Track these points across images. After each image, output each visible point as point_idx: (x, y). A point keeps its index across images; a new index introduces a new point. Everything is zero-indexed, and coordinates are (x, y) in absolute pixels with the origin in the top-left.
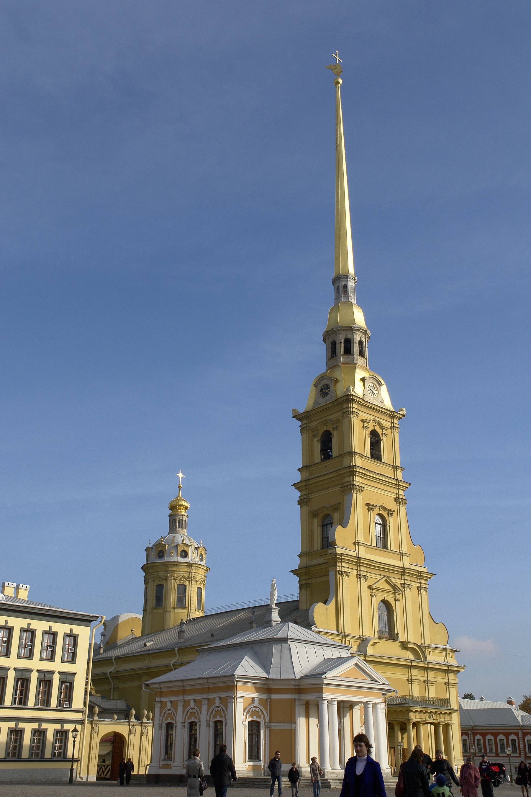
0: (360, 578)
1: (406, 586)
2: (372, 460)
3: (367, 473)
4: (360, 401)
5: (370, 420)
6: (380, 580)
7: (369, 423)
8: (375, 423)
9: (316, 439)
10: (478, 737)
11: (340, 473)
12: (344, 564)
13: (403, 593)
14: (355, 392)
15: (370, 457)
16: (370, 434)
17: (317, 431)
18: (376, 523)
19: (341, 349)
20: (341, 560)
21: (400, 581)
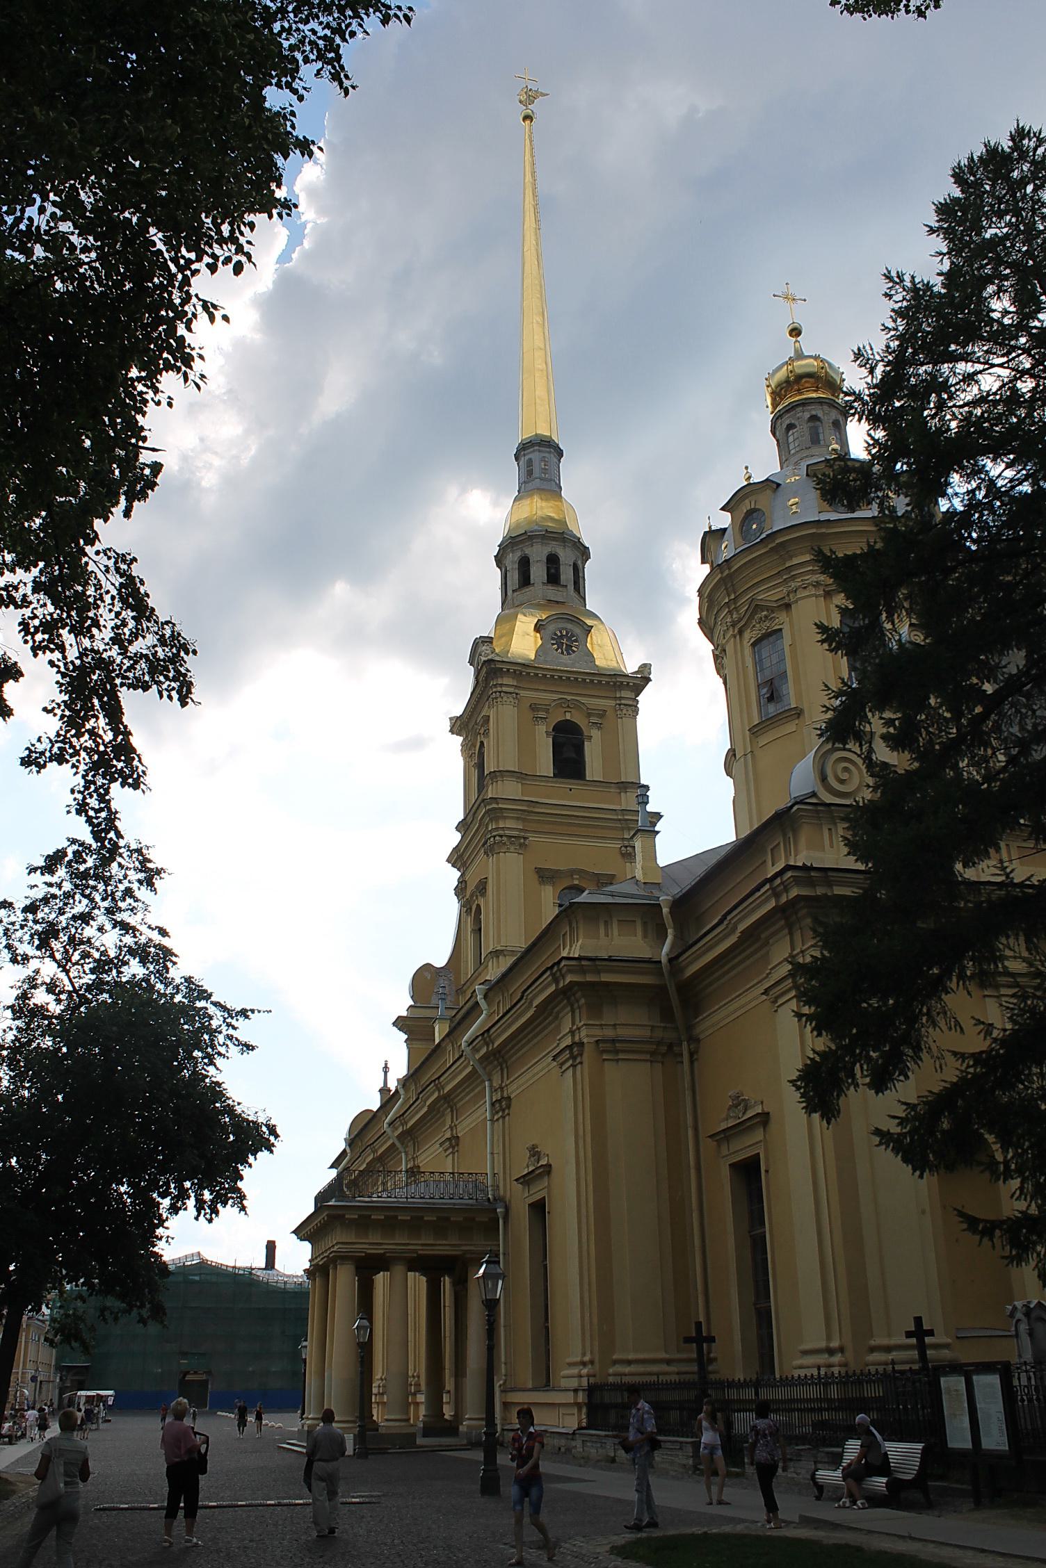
2: (555, 779)
8: (568, 706)
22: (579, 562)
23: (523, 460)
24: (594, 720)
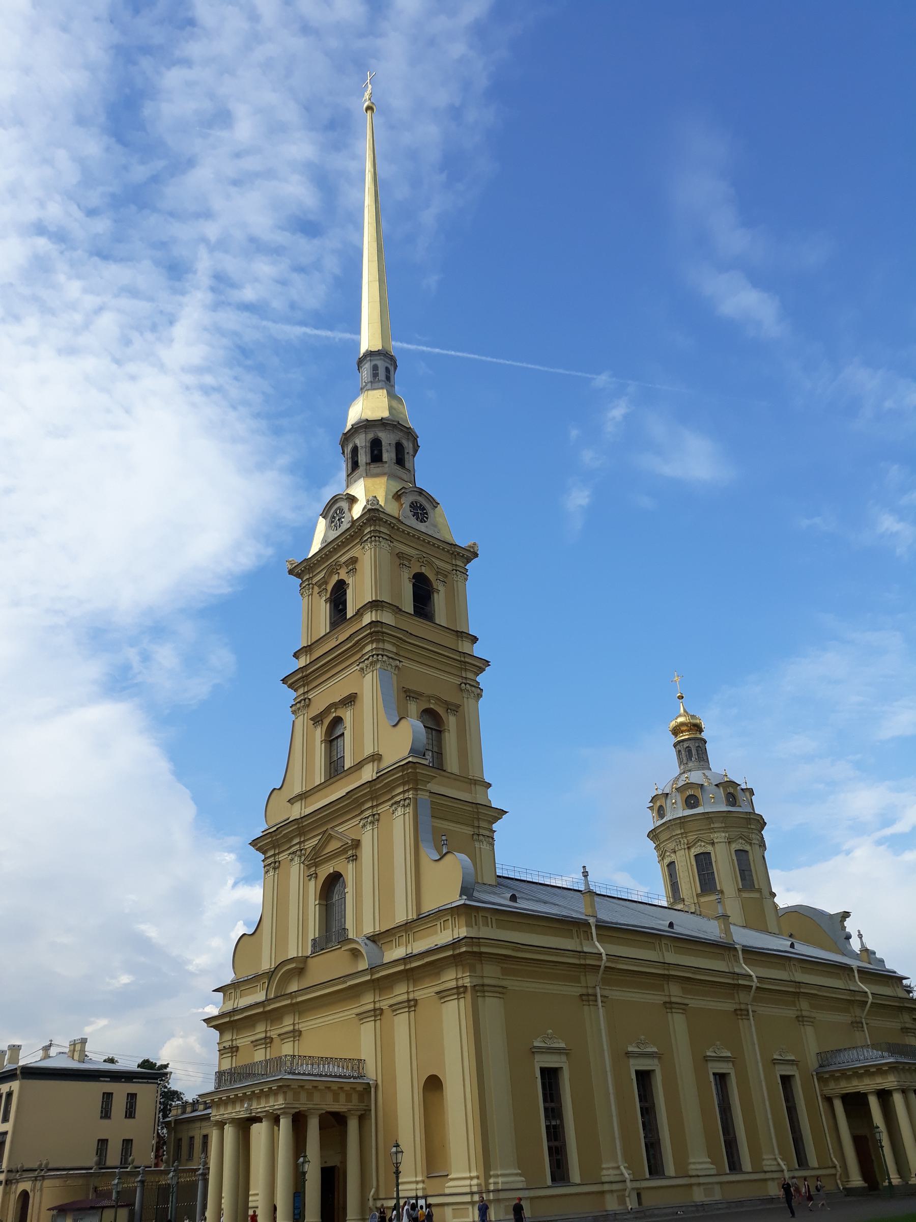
4: (393, 523)
7: (411, 560)
9: (324, 598)
11: (356, 639)
14: (381, 506)
15: (413, 613)
17: (325, 586)
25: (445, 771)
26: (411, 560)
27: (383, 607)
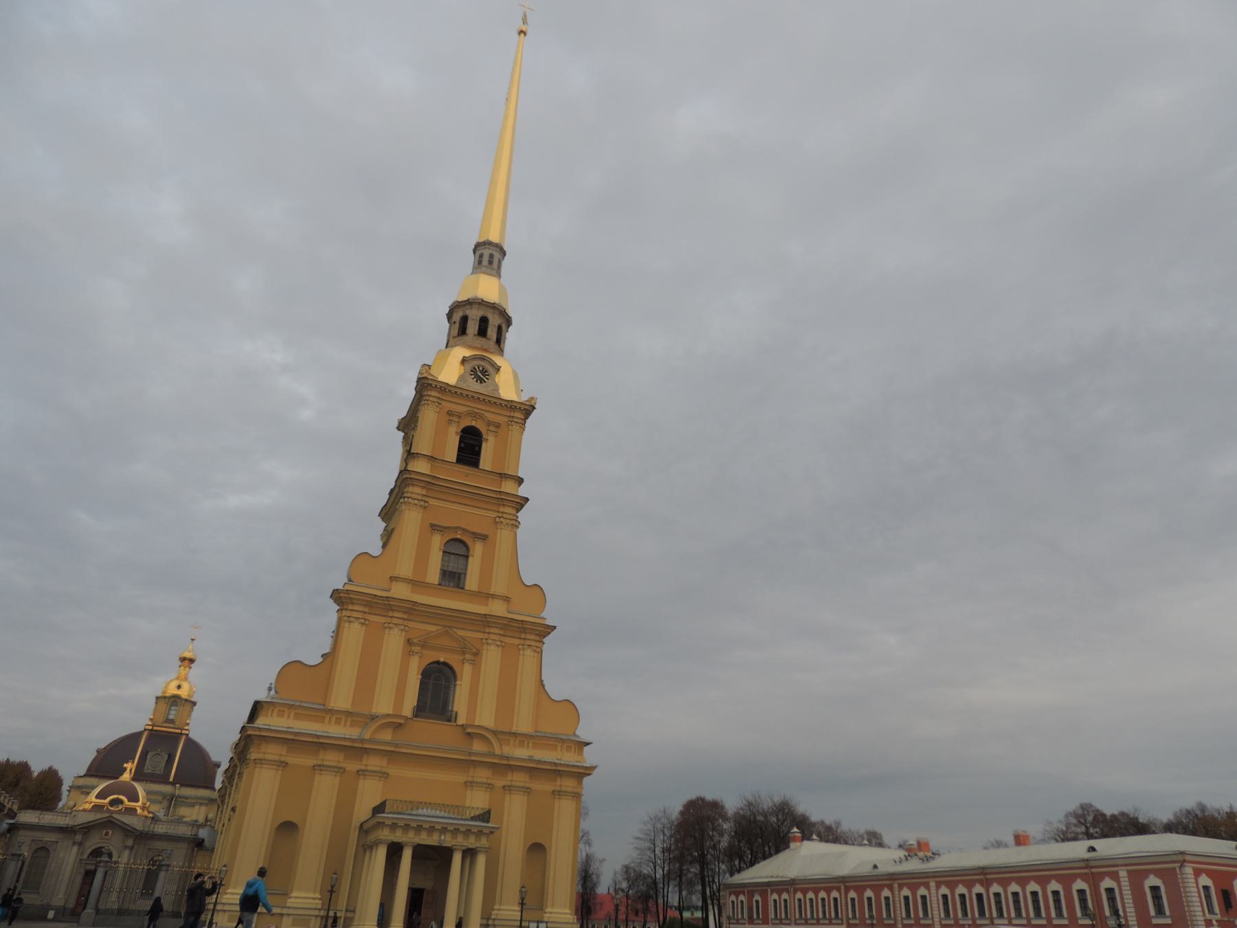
0: (390, 628)
1: (490, 642)
2: (457, 465)
3: (434, 482)
5: (462, 413)
6: (433, 632)
7: (460, 416)
8: (475, 416)
10: (799, 895)
12: (356, 608)
13: (484, 652)
15: (455, 461)
16: (462, 431)
18: (444, 552)
19: (455, 331)
20: (352, 601)
21: (480, 636)
22: (504, 327)
23: (478, 253)
24: (492, 428)
25: (463, 588)
26: (460, 416)
27: (418, 457)
